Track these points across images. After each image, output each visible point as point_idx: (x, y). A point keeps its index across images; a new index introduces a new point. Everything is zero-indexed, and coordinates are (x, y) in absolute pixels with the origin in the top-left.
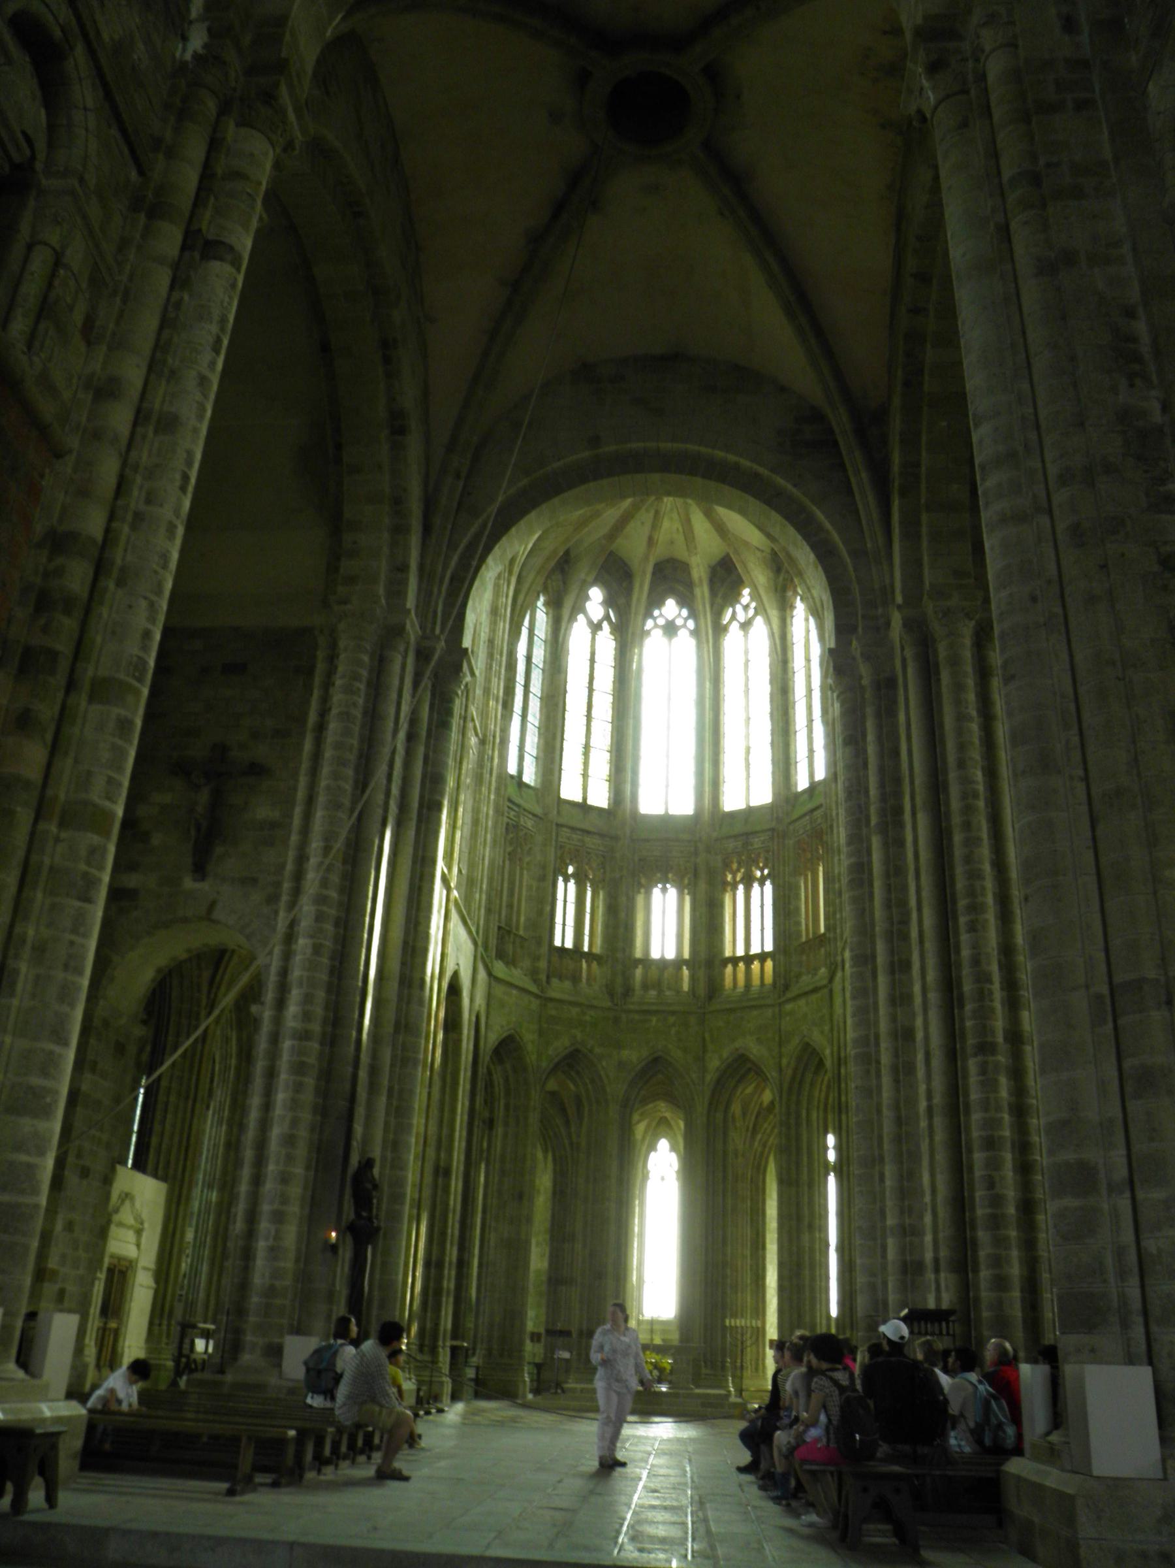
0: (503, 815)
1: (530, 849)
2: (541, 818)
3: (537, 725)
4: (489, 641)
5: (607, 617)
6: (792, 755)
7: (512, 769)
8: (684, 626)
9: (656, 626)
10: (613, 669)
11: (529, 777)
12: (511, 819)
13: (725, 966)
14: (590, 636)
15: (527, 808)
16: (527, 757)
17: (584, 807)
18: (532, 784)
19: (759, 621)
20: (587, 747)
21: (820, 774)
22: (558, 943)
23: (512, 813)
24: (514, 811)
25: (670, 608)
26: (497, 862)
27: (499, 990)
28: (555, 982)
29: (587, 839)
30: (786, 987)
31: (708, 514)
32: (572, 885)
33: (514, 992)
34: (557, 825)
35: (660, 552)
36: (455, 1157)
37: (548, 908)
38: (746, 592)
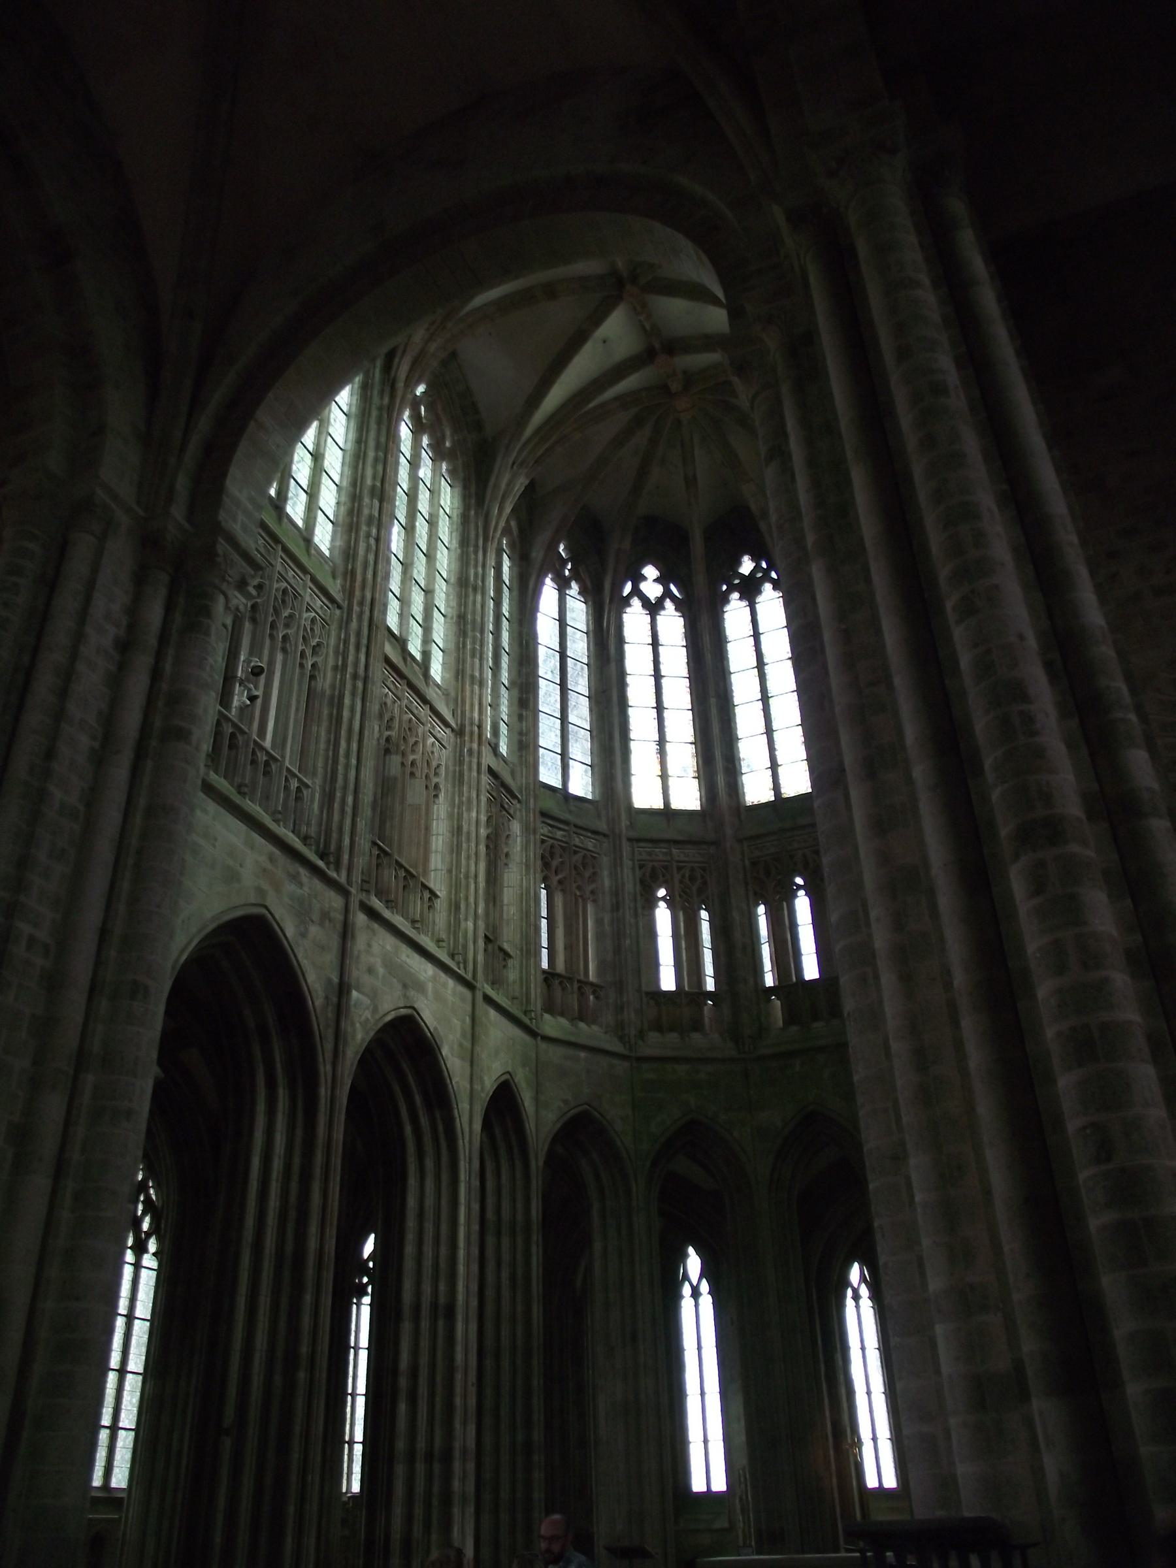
1: (594, 874)
2: (605, 835)
5: (667, 593)
8: (766, 578)
10: (685, 649)
15: (579, 822)
18: (590, 797)
23: (559, 834)
24: (560, 829)
25: (747, 566)
27: (555, 1054)
28: (653, 1037)
29: (674, 851)
33: (583, 1054)
34: (630, 840)
36: (460, 1287)
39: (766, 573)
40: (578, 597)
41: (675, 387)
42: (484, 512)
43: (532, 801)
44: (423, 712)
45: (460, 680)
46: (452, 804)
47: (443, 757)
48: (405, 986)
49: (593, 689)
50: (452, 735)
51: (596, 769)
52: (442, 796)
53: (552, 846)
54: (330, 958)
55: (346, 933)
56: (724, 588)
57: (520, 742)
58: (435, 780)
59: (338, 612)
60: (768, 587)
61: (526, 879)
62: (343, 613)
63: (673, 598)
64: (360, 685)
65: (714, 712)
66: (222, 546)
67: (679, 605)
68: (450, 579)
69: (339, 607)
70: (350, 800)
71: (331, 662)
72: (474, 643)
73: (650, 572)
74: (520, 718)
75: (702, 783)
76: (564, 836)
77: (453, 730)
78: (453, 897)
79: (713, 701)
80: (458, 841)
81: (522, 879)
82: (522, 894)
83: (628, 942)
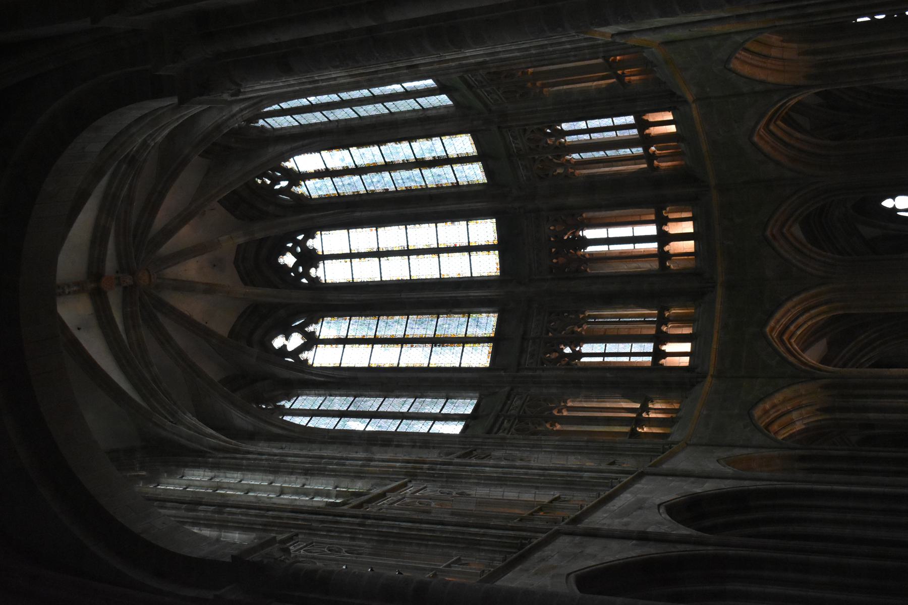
0: (503, 438)
2: (512, 389)
3: (412, 400)
4: (306, 474)
5: (301, 329)
6: (414, 114)
7: (455, 428)
8: (303, 243)
9: (306, 274)
11: (466, 407)
12: (511, 427)
13: (658, 167)
14: (321, 347)
16: (444, 411)
17: (497, 341)
18: (475, 401)
19: (289, 164)
20: (436, 341)
21: (430, 83)
22: (649, 359)
23: (506, 425)
24: (503, 423)
25: (289, 260)
26: (557, 443)
30: (673, 94)
31: (168, 232)
32: (586, 348)
35: (229, 278)
37: (608, 375)
38: (259, 181)
39: (297, 243)
40: (292, 401)
41: (129, 281)
42: (211, 451)
43: (475, 440)
44: (391, 498)
45: (365, 475)
46: (478, 484)
47: (431, 490)
48: (640, 508)
49: (378, 393)
50: (413, 482)
51: (451, 394)
52: (468, 492)
53: (517, 430)
54: (615, 545)
55: (594, 534)
56: (304, 281)
57: (420, 447)
58: (454, 494)
59: (300, 536)
60: (310, 243)
61: (545, 448)
62: (302, 533)
63: (307, 324)
64: (369, 522)
65: (415, 295)
66: (256, 557)
67: (315, 319)
68: (269, 480)
69: (297, 535)
70: (473, 530)
71: (347, 542)
72: (331, 464)
73: (278, 342)
74: (397, 446)
75: (475, 310)
76: (509, 421)
77: (410, 481)
78: (560, 486)
79: (404, 295)
80: (510, 481)
81: (544, 451)
82: (558, 452)
83: (608, 375)
